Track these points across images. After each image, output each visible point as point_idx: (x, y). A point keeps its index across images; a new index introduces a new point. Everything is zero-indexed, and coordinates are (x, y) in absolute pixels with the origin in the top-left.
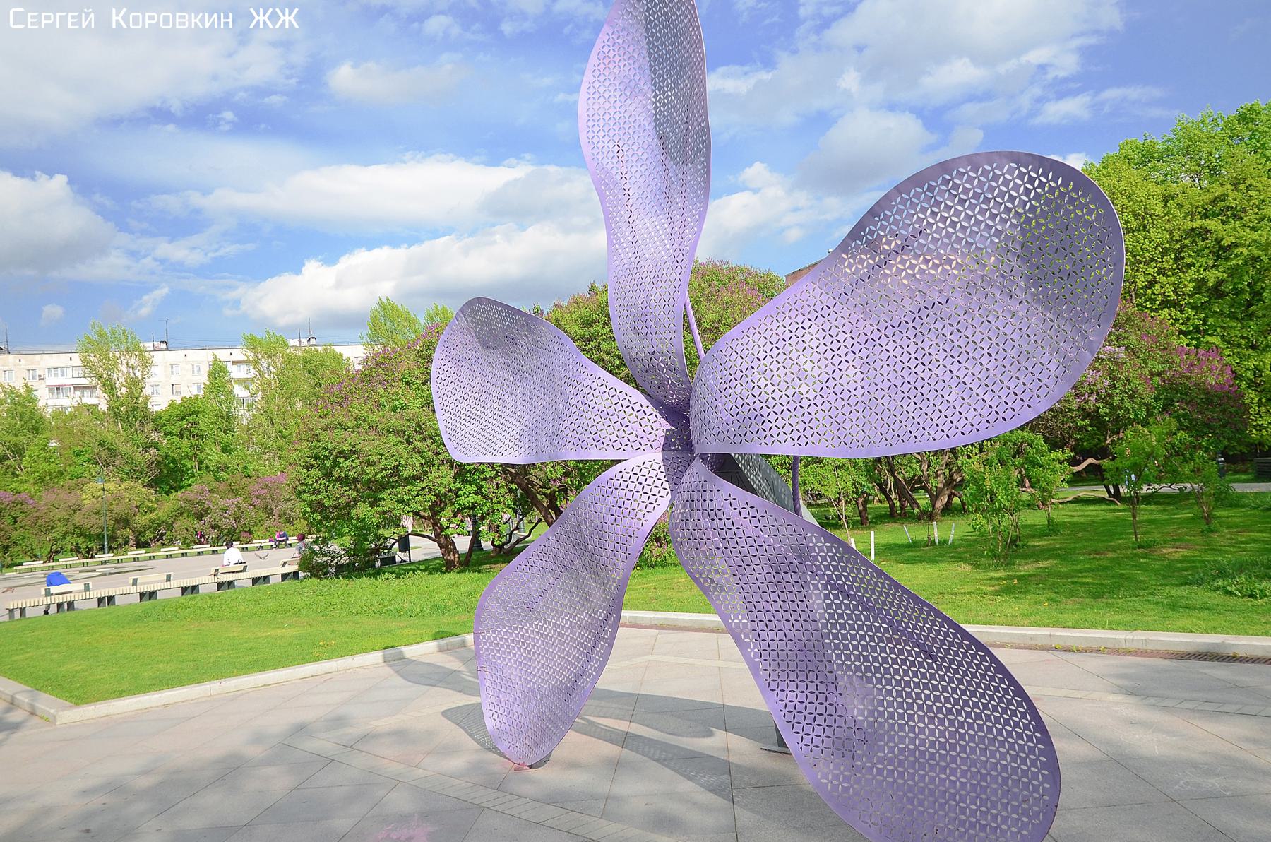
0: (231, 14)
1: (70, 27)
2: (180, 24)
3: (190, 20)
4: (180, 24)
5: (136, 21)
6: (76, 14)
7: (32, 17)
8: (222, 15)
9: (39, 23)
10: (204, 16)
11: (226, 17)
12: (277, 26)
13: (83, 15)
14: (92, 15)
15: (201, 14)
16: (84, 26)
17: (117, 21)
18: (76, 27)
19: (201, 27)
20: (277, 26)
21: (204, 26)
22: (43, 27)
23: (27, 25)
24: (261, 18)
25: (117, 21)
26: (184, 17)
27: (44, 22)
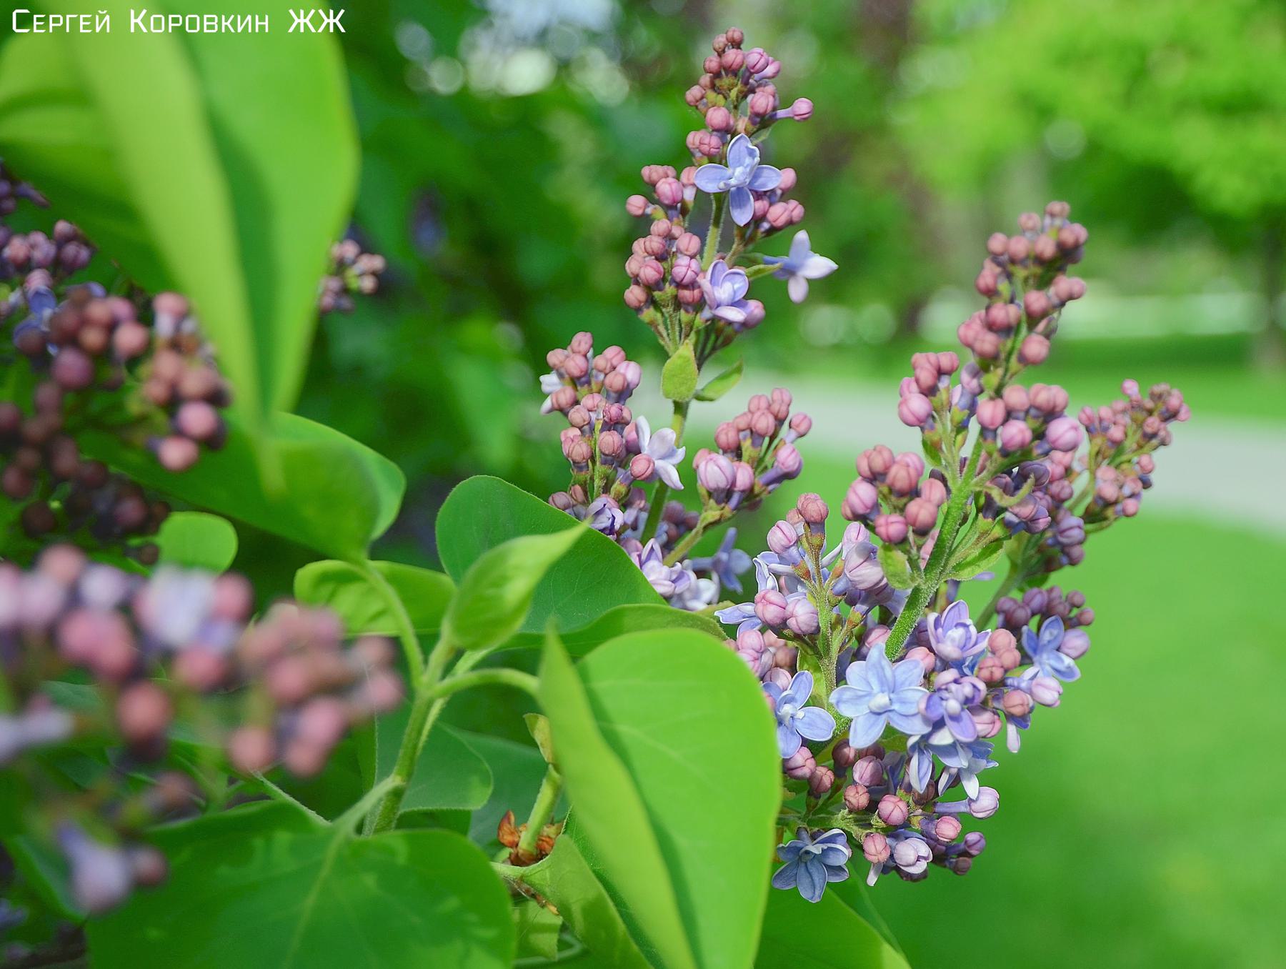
0: (267, 17)
1: (82, 31)
2: (209, 27)
3: (220, 23)
4: (209, 27)
6: (89, 16)
7: (38, 20)
8: (257, 17)
10: (235, 19)
11: (262, 19)
13: (97, 17)
14: (107, 18)
15: (233, 16)
16: (98, 30)
17: (136, 24)
18: (89, 31)
19: (233, 31)
20: (320, 30)
21: (236, 29)
22: (51, 31)
24: (302, 21)
25: (136, 24)
26: (213, 20)
27: (51, 25)
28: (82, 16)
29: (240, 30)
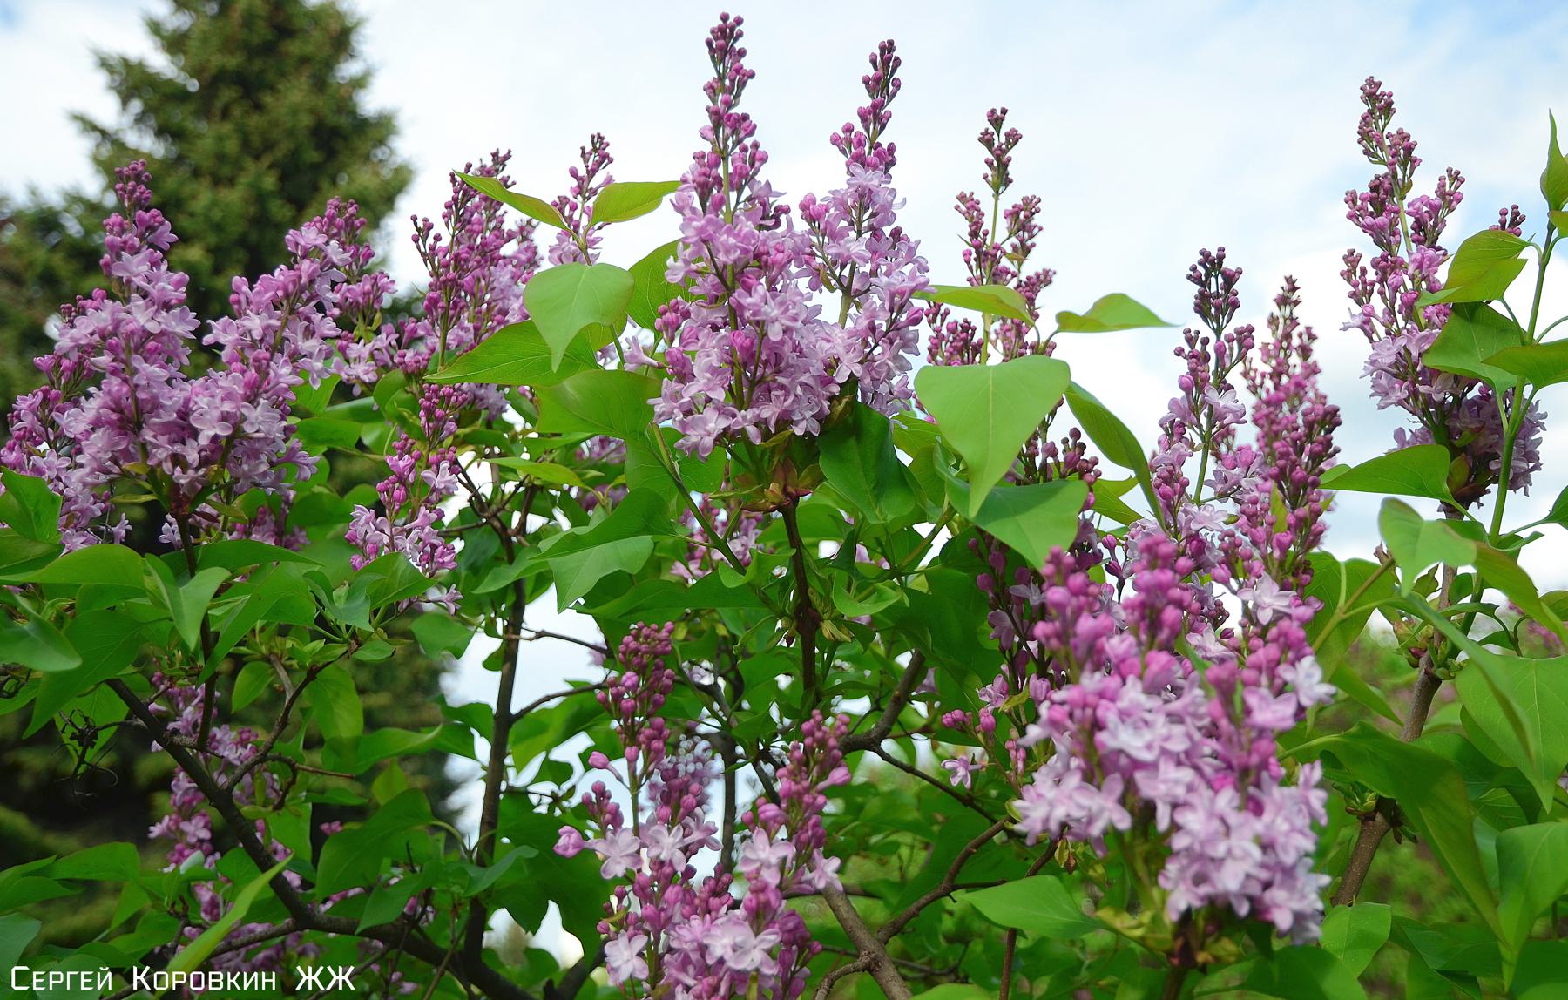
1: (83, 988)
2: (215, 984)
3: (225, 980)
4: (215, 984)
7: (38, 977)
9: (46, 984)
10: (242, 975)
12: (329, 988)
16: (99, 987)
20: (329, 988)
21: (241, 984)
23: (30, 983)
24: (310, 978)
28: (83, 973)
29: (246, 987)
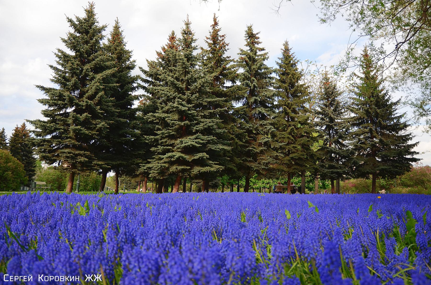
2: (62, 280)
4: (62, 280)
5: (46, 278)
9: (14, 279)
11: (77, 277)
16: (29, 280)
21: (69, 280)
23: (9, 279)
24: (89, 278)
27: (15, 279)
29: (71, 280)
